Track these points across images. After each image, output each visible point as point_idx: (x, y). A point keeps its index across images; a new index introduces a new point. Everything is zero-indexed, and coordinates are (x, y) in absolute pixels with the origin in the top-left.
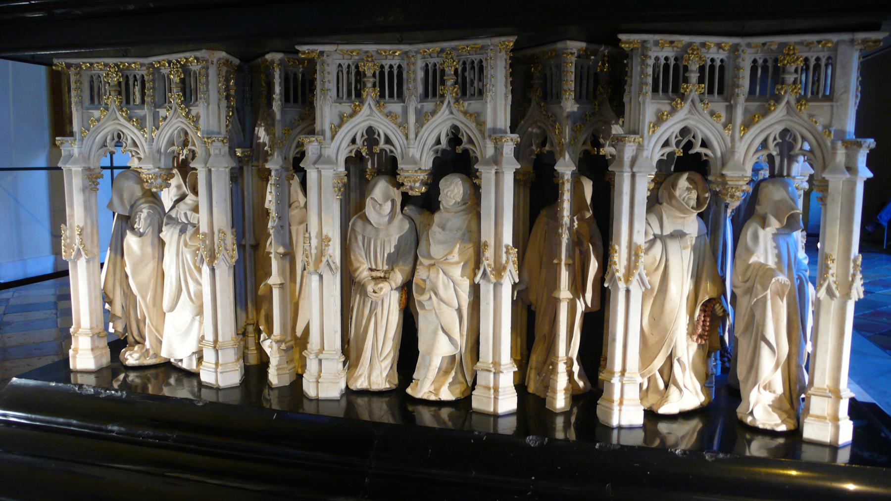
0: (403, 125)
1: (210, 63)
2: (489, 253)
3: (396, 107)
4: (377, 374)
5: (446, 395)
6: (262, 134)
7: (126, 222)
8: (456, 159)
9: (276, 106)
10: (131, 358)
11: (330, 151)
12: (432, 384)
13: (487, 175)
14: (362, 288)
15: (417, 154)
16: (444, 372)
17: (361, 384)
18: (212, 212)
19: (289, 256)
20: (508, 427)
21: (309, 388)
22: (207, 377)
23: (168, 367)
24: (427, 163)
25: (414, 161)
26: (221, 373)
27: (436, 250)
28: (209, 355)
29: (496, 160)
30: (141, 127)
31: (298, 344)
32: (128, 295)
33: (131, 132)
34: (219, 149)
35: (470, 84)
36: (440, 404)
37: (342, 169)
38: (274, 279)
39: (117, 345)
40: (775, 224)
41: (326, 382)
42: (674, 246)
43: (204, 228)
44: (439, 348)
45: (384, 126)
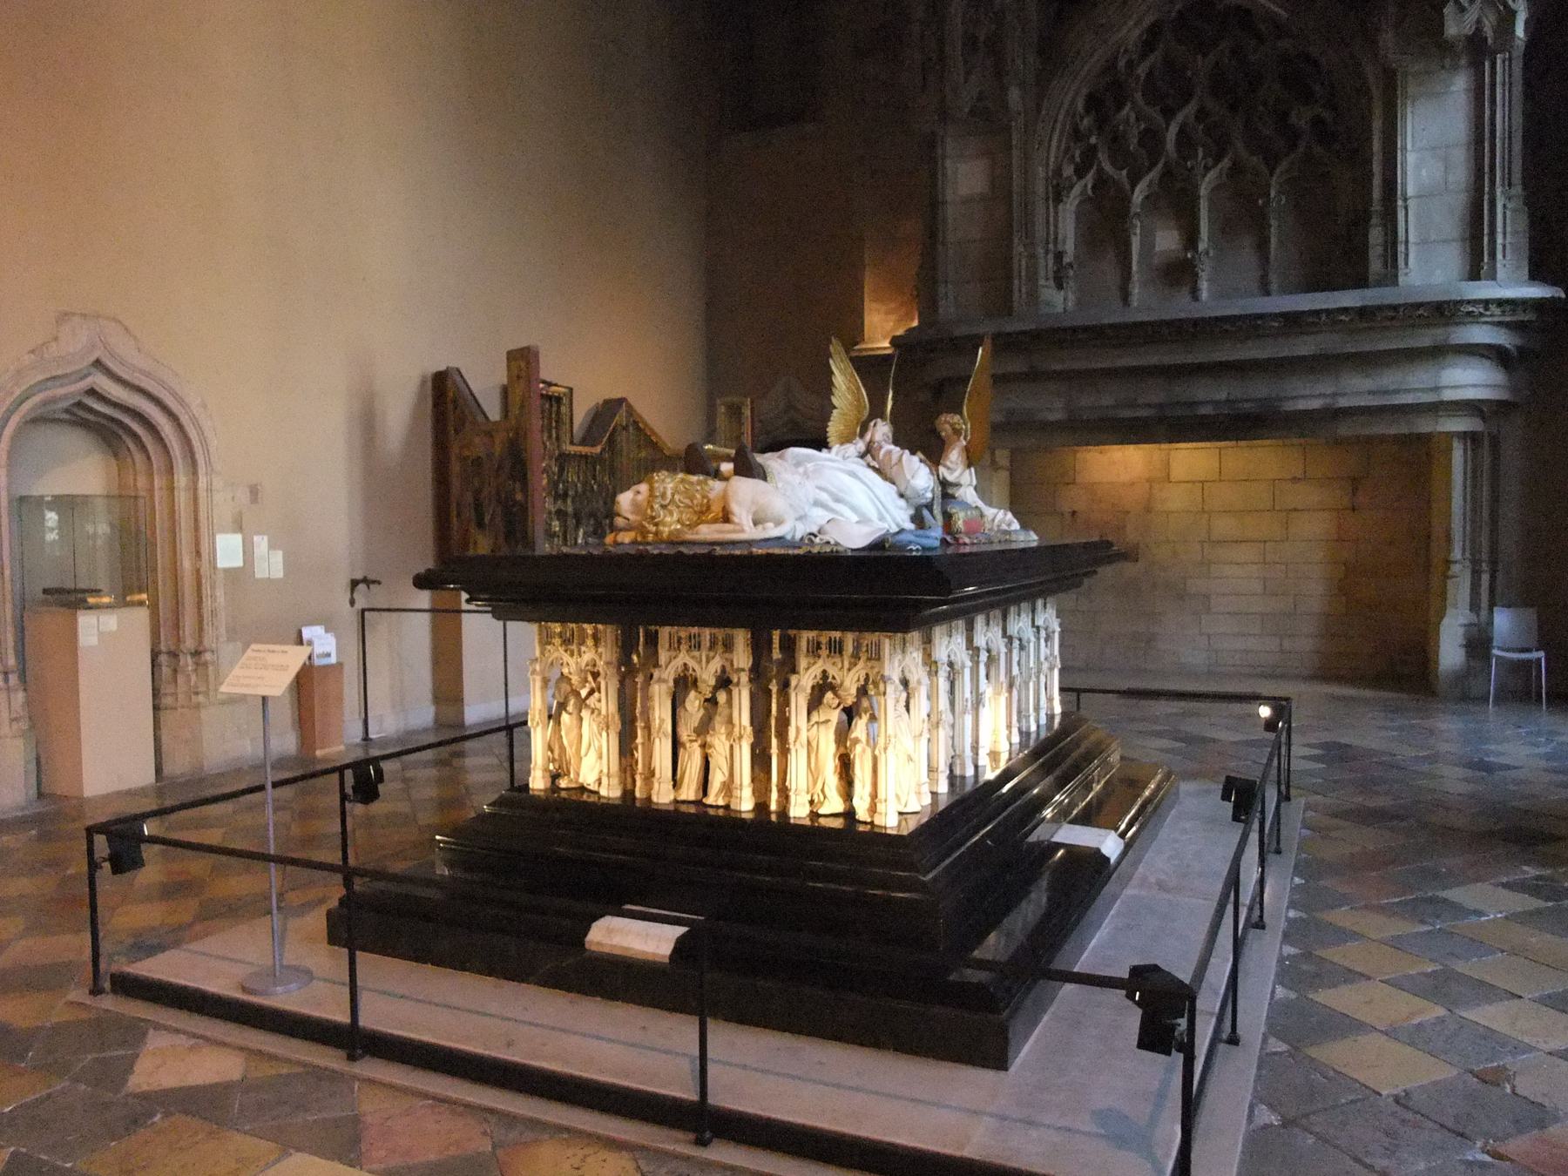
0: (700, 662)
1: (609, 632)
2: (736, 730)
3: (696, 653)
4: (689, 792)
5: (721, 802)
6: (635, 658)
7: (562, 706)
8: (724, 682)
9: (641, 648)
10: (563, 783)
11: (665, 676)
12: (714, 798)
13: (735, 692)
14: (683, 745)
15: (708, 675)
16: (720, 791)
17: (683, 797)
18: (606, 703)
19: (648, 728)
20: (749, 816)
21: (655, 799)
22: (603, 792)
23: (582, 789)
24: (712, 682)
25: (704, 681)
26: (610, 791)
27: (717, 726)
28: (605, 781)
29: (738, 684)
30: (572, 655)
31: (650, 774)
32: (562, 748)
33: (566, 658)
34: (612, 671)
35: (728, 646)
36: (718, 807)
37: (671, 683)
38: (639, 740)
39: (555, 777)
40: (865, 718)
41: (663, 795)
42: (822, 728)
43: (604, 712)
44: (717, 778)
45: (692, 664)
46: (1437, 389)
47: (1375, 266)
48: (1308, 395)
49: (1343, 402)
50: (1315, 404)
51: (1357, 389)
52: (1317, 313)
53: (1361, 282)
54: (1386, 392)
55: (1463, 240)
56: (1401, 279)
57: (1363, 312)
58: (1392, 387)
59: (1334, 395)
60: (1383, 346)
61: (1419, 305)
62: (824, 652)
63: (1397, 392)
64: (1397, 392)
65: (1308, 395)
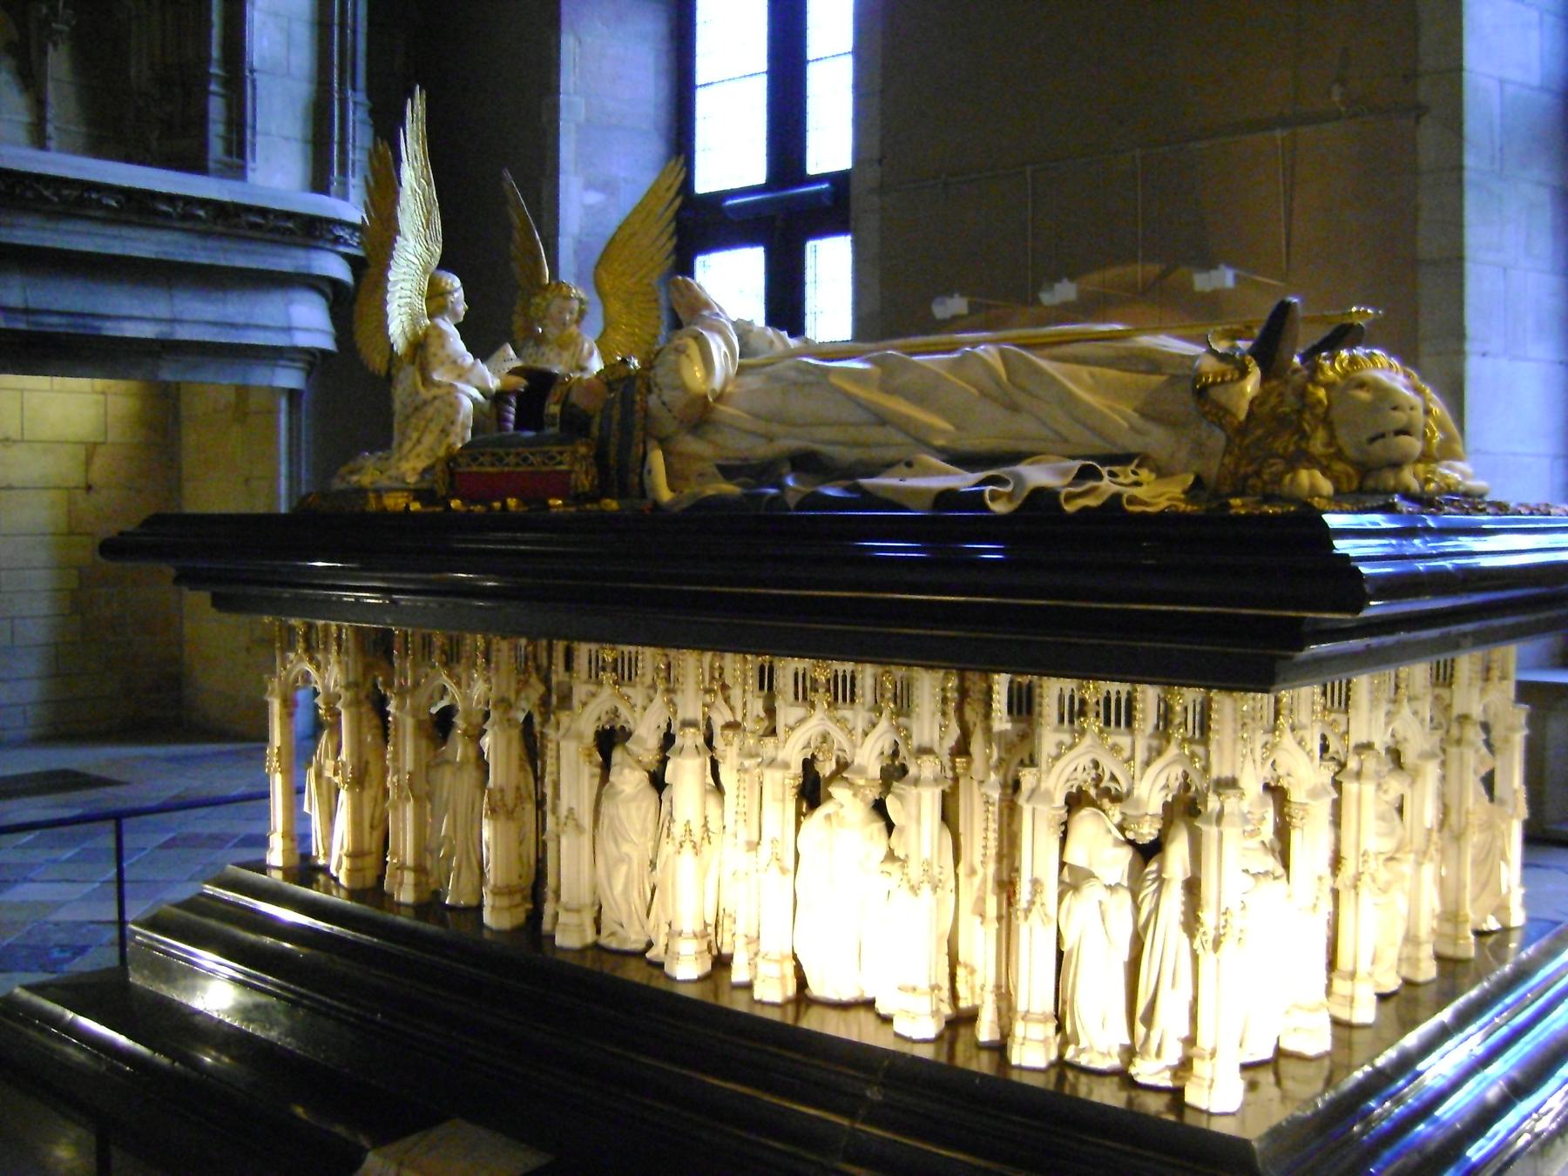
46: (289, 330)
47: (216, 148)
48: (137, 315)
49: (184, 333)
50: (147, 331)
51: (198, 316)
52: (171, 199)
53: (195, 164)
54: (233, 325)
55: (306, 142)
56: (250, 174)
57: (221, 211)
58: (241, 320)
59: (173, 321)
60: (241, 261)
61: (289, 215)
62: (1093, 724)
63: (247, 326)
64: (247, 326)
65: (137, 315)
